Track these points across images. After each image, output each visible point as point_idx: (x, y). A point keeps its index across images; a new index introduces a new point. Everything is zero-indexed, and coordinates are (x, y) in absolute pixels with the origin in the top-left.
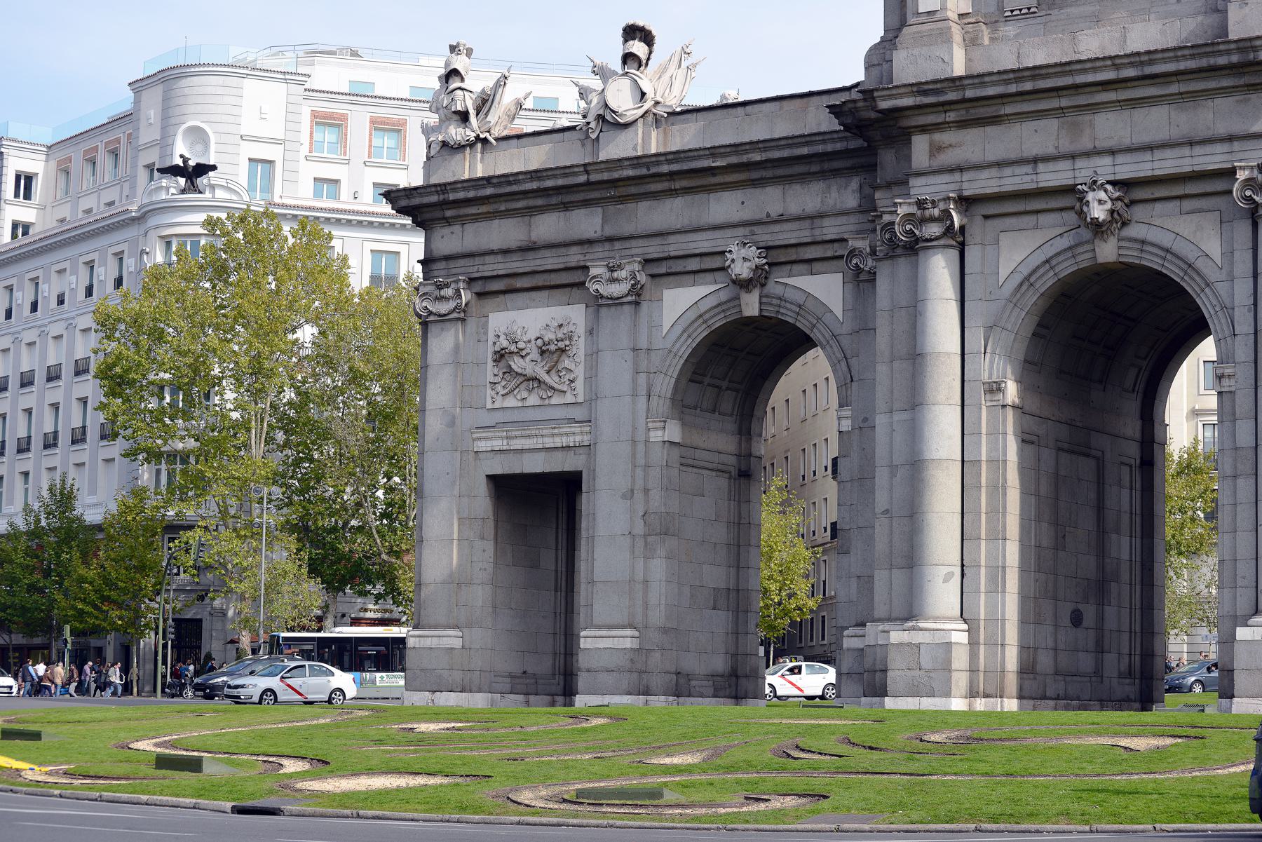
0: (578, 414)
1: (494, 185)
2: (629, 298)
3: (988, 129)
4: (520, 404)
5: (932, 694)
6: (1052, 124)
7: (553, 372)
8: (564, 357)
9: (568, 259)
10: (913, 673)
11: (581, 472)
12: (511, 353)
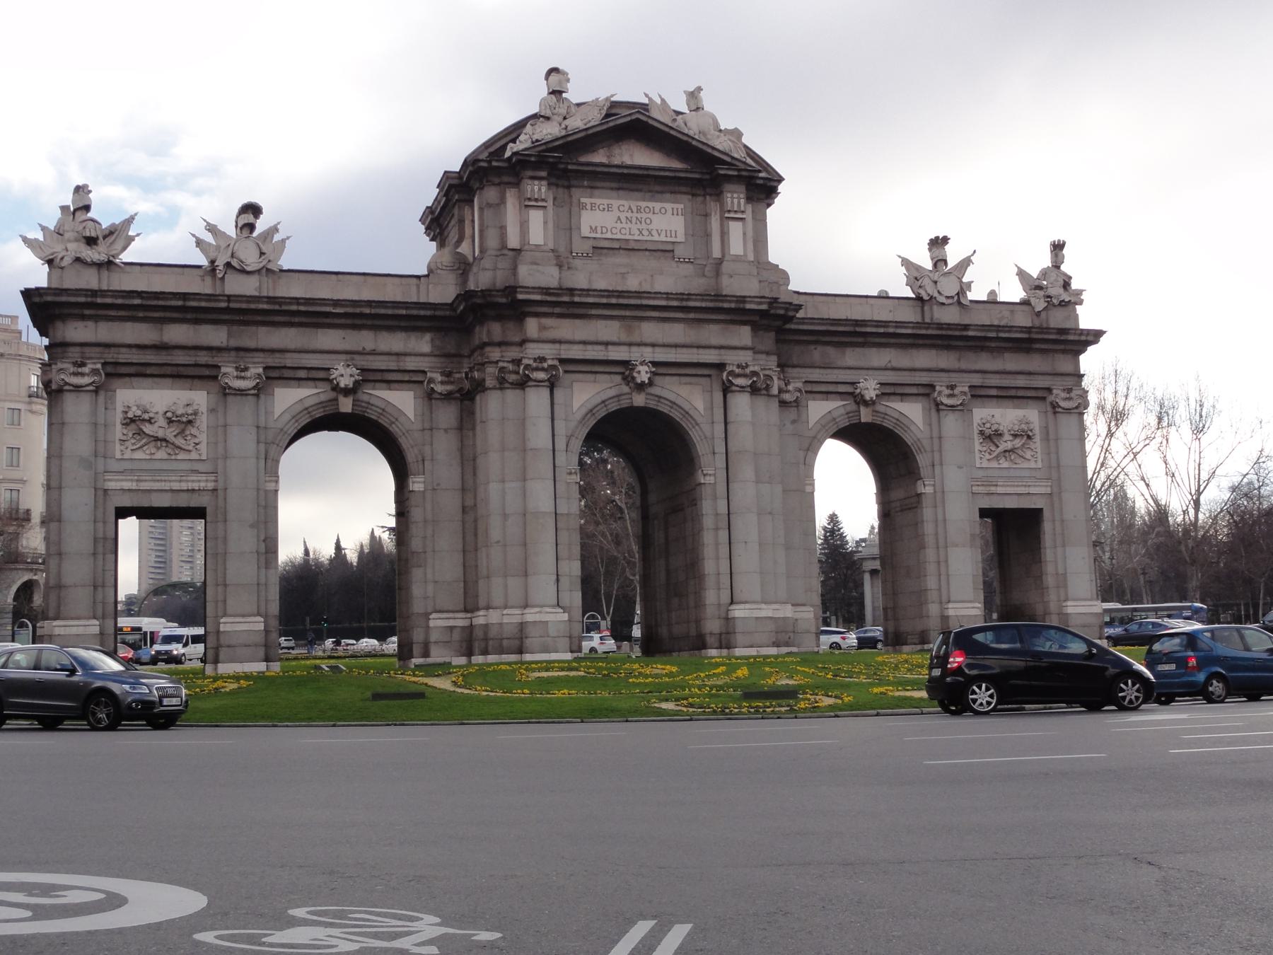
1: (142, 298)
2: (253, 392)
3: (577, 322)
4: (148, 457)
6: (615, 324)
7: (179, 437)
8: (190, 427)
9: (198, 359)
10: (543, 639)
11: (205, 508)
12: (144, 420)
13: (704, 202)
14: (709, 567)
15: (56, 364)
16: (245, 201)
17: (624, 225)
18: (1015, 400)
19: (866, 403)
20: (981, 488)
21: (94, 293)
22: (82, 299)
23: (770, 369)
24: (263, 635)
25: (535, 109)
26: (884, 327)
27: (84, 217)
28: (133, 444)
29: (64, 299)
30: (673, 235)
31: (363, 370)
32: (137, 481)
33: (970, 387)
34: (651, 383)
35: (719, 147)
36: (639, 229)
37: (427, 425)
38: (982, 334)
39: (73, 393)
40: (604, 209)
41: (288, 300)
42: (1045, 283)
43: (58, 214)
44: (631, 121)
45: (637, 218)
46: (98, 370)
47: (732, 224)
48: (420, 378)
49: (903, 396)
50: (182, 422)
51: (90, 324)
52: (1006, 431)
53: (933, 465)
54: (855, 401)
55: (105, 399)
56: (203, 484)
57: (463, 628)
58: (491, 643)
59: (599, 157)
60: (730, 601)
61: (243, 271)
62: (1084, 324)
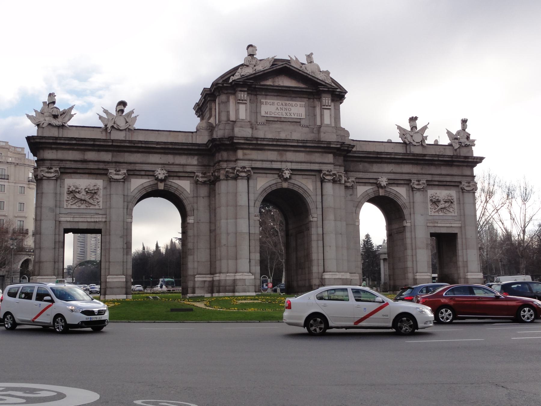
0: (100, 212)
1: (76, 141)
2: (122, 180)
3: (259, 152)
4: (78, 208)
5: (249, 292)
6: (276, 153)
8: (95, 195)
9: (99, 166)
10: (244, 286)
12: (76, 192)
13: (313, 102)
14: (314, 256)
15: (40, 168)
16: (120, 100)
18: (446, 187)
19: (382, 187)
20: (430, 224)
21: (56, 138)
22: (51, 141)
23: (341, 172)
24: (125, 283)
25: (242, 62)
26: (390, 155)
27: (52, 107)
28: (72, 202)
29: (44, 141)
30: (300, 115)
31: (169, 172)
32: (73, 217)
33: (426, 181)
34: (290, 178)
35: (320, 78)
36: (286, 113)
37: (195, 195)
38: (432, 158)
39: (47, 180)
40: (271, 104)
41: (137, 142)
42: (459, 137)
43: (42, 105)
44: (283, 67)
45: (285, 108)
46: (57, 171)
47: (325, 111)
48: (192, 175)
49: (398, 185)
50: (92, 193)
51: (54, 151)
52: (442, 200)
53: (410, 214)
54: (377, 186)
55: (60, 182)
56: (100, 219)
57: (210, 281)
58: (221, 288)
59: (269, 82)
60: (323, 271)
61: (119, 130)
62: (475, 155)
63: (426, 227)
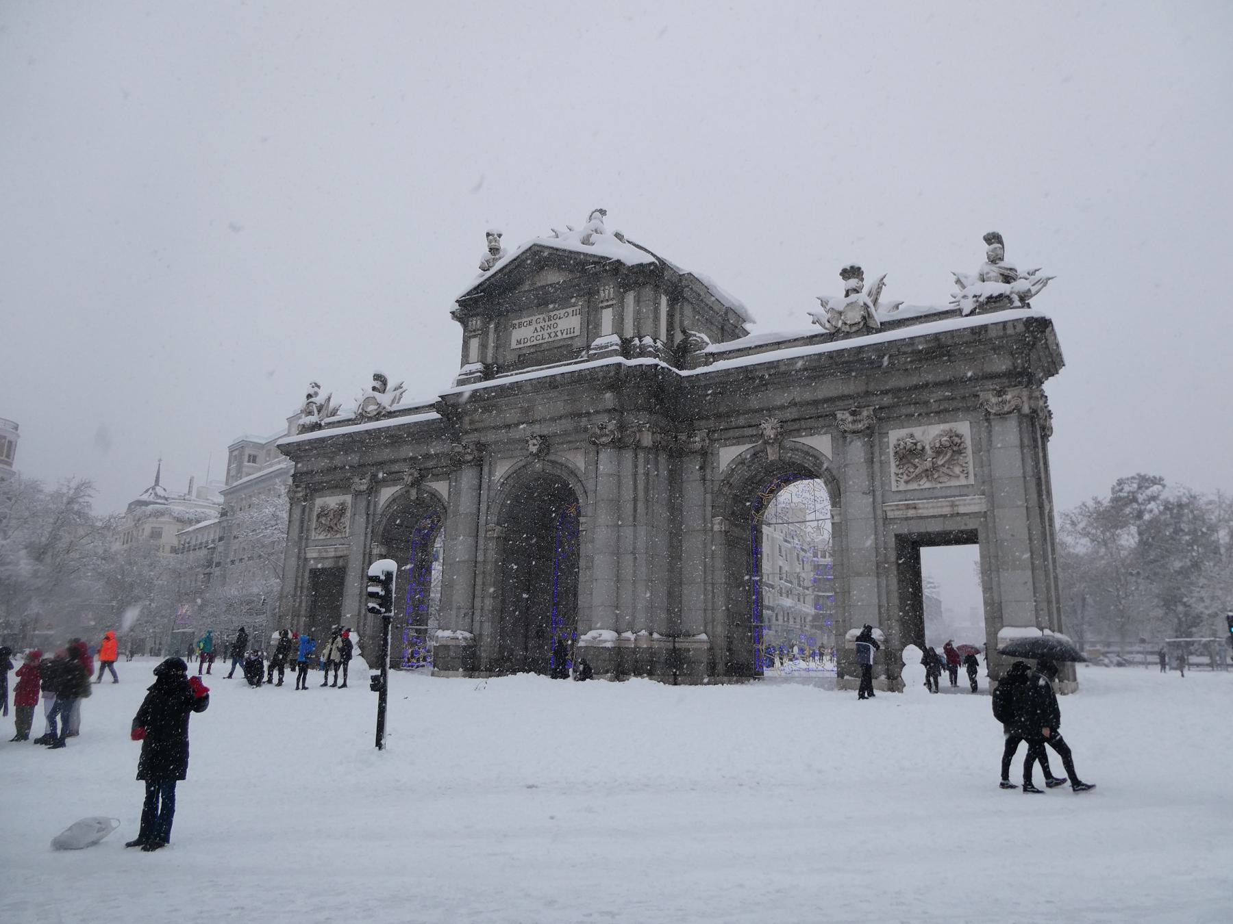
4: (324, 538)
17: (539, 333)
30: (572, 332)
49: (811, 431)
52: (927, 447)
63: (881, 522)
